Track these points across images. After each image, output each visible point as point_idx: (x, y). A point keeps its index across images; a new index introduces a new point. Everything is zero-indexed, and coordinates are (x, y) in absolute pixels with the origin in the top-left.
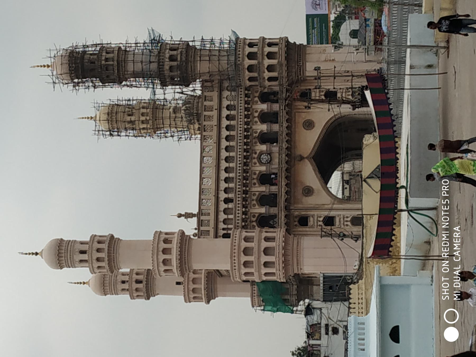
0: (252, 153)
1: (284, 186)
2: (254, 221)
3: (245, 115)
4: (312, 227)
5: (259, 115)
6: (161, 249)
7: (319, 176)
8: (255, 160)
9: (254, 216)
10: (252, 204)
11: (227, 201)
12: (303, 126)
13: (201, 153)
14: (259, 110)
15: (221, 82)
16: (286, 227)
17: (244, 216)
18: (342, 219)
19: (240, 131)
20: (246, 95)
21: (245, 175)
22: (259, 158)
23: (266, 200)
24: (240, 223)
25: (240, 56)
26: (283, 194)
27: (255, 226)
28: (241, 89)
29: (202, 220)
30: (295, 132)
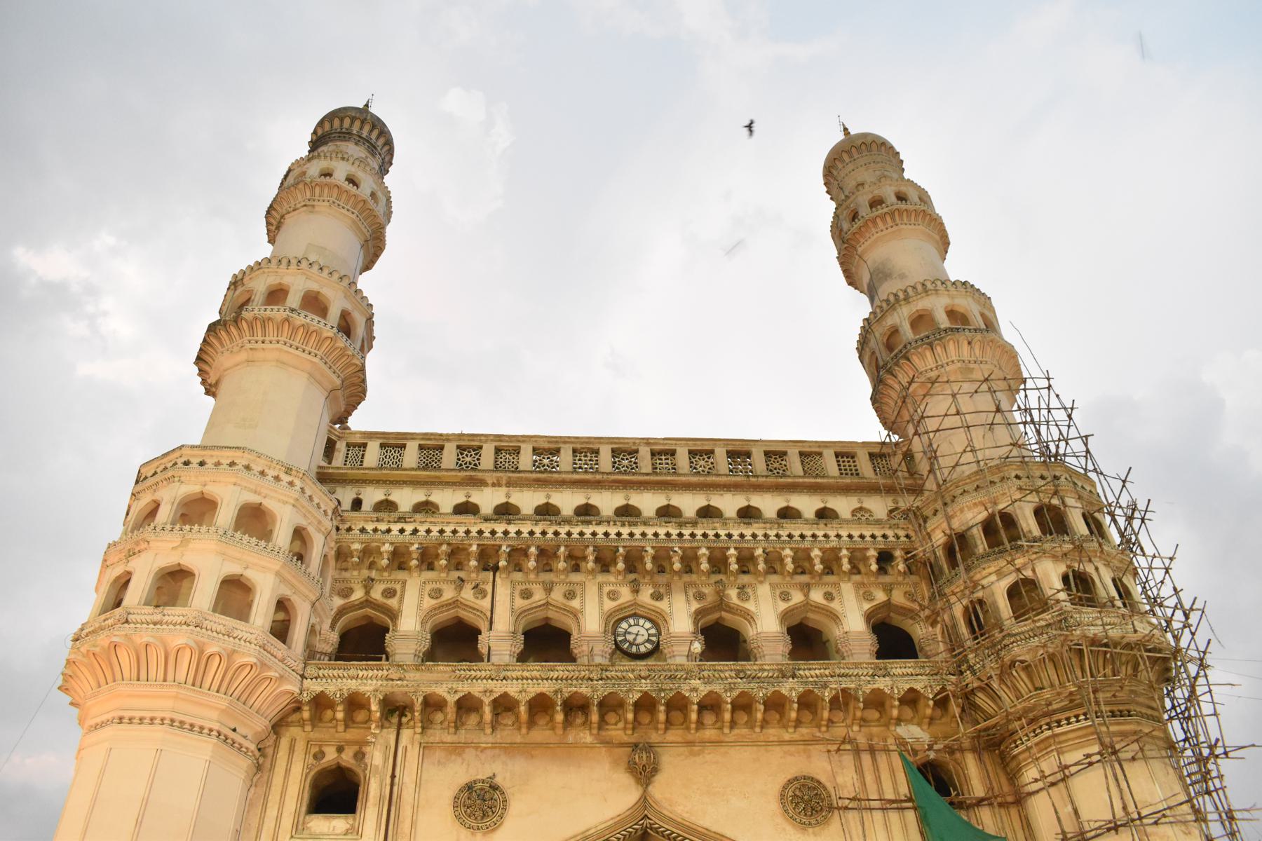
0: (655, 585)
1: (499, 688)
2: (367, 593)
3: (807, 552)
4: (298, 827)
5: (818, 608)
6: (287, 280)
9: (389, 593)
10: (444, 587)
12: (796, 779)
13: (647, 441)
14: (835, 605)
15: (917, 490)
16: (306, 697)
17: (387, 548)
20: (885, 558)
22: (634, 614)
23: (455, 639)
26: (464, 688)
28: (907, 536)
29: (404, 446)
30: (768, 743)
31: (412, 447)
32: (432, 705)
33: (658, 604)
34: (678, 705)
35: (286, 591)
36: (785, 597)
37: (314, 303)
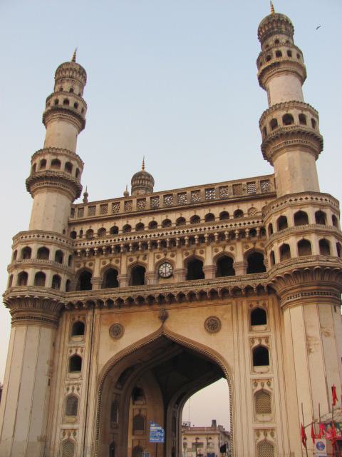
5: (229, 253)
7: (137, 346)
8: (162, 257)
9: (91, 265)
11: (115, 230)
13: (176, 190)
14: (233, 252)
18: (76, 382)
19: (201, 230)
20: (253, 231)
21: (140, 243)
22: (165, 262)
23: (111, 277)
24: (79, 248)
25: (299, 201)
26: (107, 296)
27: (78, 267)
31: (98, 206)
32: (100, 302)
33: (172, 259)
34: (171, 296)
35: (55, 273)
36: (216, 251)
37: (56, 163)
